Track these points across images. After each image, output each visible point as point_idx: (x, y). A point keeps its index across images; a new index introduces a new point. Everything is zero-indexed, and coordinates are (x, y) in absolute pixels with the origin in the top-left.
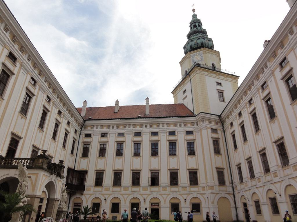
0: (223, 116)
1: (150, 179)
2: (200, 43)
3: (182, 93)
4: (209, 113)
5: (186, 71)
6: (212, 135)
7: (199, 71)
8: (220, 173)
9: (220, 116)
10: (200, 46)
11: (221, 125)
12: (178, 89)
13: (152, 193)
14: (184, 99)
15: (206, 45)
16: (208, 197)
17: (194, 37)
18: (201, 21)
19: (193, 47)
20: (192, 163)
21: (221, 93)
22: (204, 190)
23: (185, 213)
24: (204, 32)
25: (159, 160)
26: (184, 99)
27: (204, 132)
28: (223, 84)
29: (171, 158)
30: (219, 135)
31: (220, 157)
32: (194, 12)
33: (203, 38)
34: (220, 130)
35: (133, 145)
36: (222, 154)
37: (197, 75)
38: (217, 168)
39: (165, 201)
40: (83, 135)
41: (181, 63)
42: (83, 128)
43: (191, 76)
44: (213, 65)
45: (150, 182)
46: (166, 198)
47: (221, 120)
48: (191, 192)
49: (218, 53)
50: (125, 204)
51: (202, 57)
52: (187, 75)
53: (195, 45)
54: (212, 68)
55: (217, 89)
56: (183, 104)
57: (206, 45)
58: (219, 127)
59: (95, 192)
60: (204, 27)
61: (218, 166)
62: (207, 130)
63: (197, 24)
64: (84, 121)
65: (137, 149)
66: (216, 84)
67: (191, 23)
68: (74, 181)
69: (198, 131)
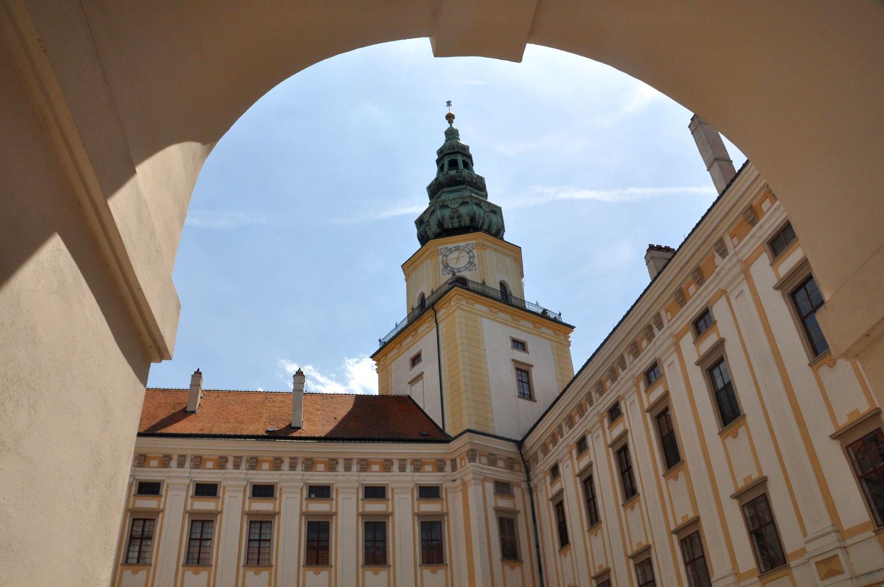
0: (529, 443)
2: (468, 215)
3: (408, 363)
4: (491, 432)
5: (422, 297)
7: (464, 302)
9: (520, 444)
10: (468, 223)
11: (523, 469)
12: (393, 349)
14: (412, 382)
15: (483, 223)
17: (451, 196)
18: (472, 151)
19: (448, 225)
21: (523, 373)
24: (479, 185)
25: (330, 577)
26: (412, 382)
27: (474, 492)
28: (530, 347)
29: (371, 572)
30: (518, 501)
31: (518, 569)
32: (451, 122)
34: (518, 485)
35: (245, 523)
36: (523, 559)
37: (457, 312)
41: (409, 267)
43: (441, 313)
44: (503, 285)
47: (521, 453)
49: (515, 252)
51: (474, 257)
52: (423, 309)
53: (451, 218)
54: (499, 295)
55: (513, 360)
56: (409, 397)
57: (483, 223)
58: (515, 477)
60: (478, 169)
62: (483, 486)
63: (460, 159)
65: (260, 540)
66: (509, 344)
67: (442, 154)
69: (455, 488)
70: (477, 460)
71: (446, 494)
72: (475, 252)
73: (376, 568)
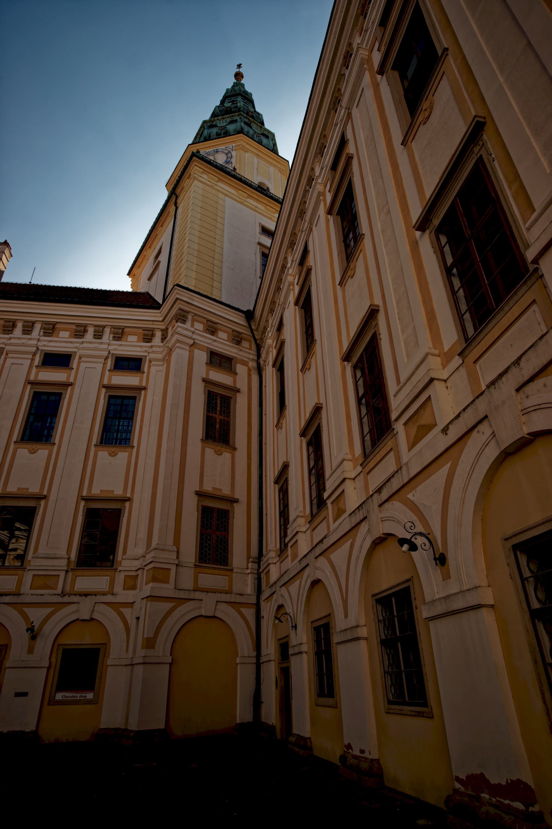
6: (207, 373)
8: (214, 521)
11: (254, 347)
16: (138, 618)
20: (110, 473)
22: (134, 588)
23: (25, 694)
31: (227, 456)
33: (247, 120)
34: (245, 363)
36: (237, 446)
38: (199, 494)
48: (70, 595)
58: (244, 353)
61: (208, 487)
66: (258, 229)
70: (189, 323)
71: (149, 367)
72: (234, 153)
73: (34, 446)
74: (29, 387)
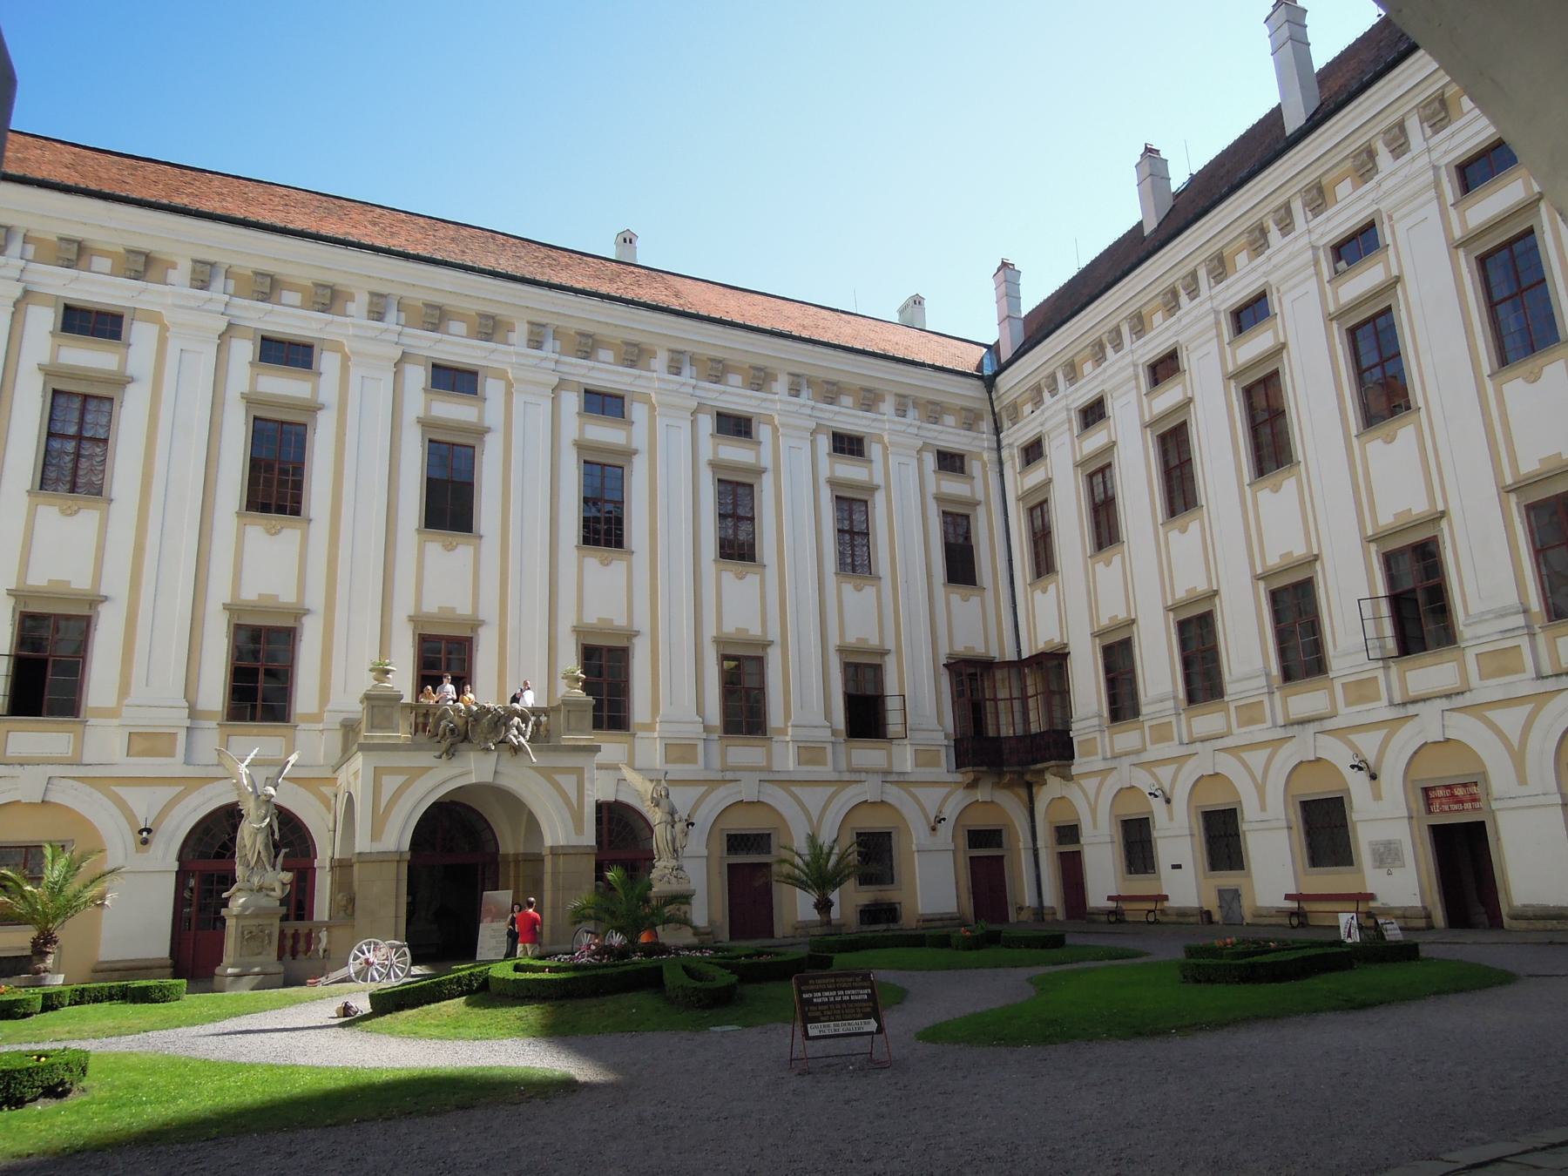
1: (1385, 609)
13: (1411, 709)
39: (1518, 758)
40: (1013, 458)
42: (1006, 424)
45: (1388, 628)
46: (1499, 732)
50: (1263, 808)
59: (1119, 756)
64: (989, 383)
68: (1033, 716)
74: (1461, 252)
